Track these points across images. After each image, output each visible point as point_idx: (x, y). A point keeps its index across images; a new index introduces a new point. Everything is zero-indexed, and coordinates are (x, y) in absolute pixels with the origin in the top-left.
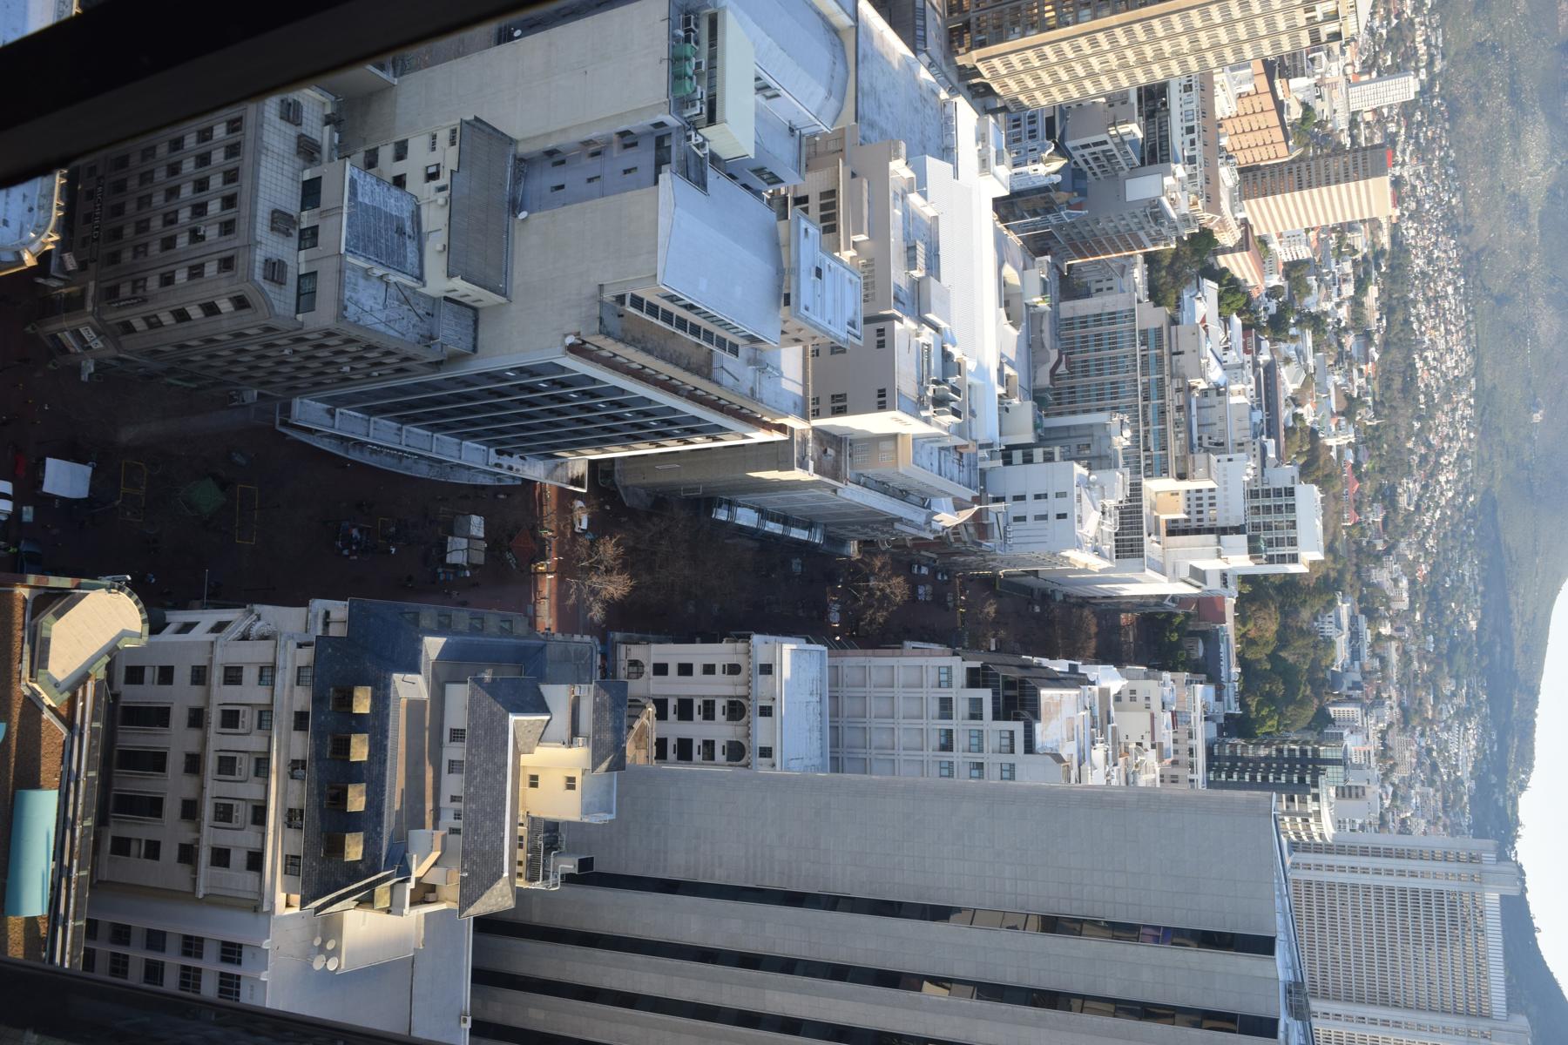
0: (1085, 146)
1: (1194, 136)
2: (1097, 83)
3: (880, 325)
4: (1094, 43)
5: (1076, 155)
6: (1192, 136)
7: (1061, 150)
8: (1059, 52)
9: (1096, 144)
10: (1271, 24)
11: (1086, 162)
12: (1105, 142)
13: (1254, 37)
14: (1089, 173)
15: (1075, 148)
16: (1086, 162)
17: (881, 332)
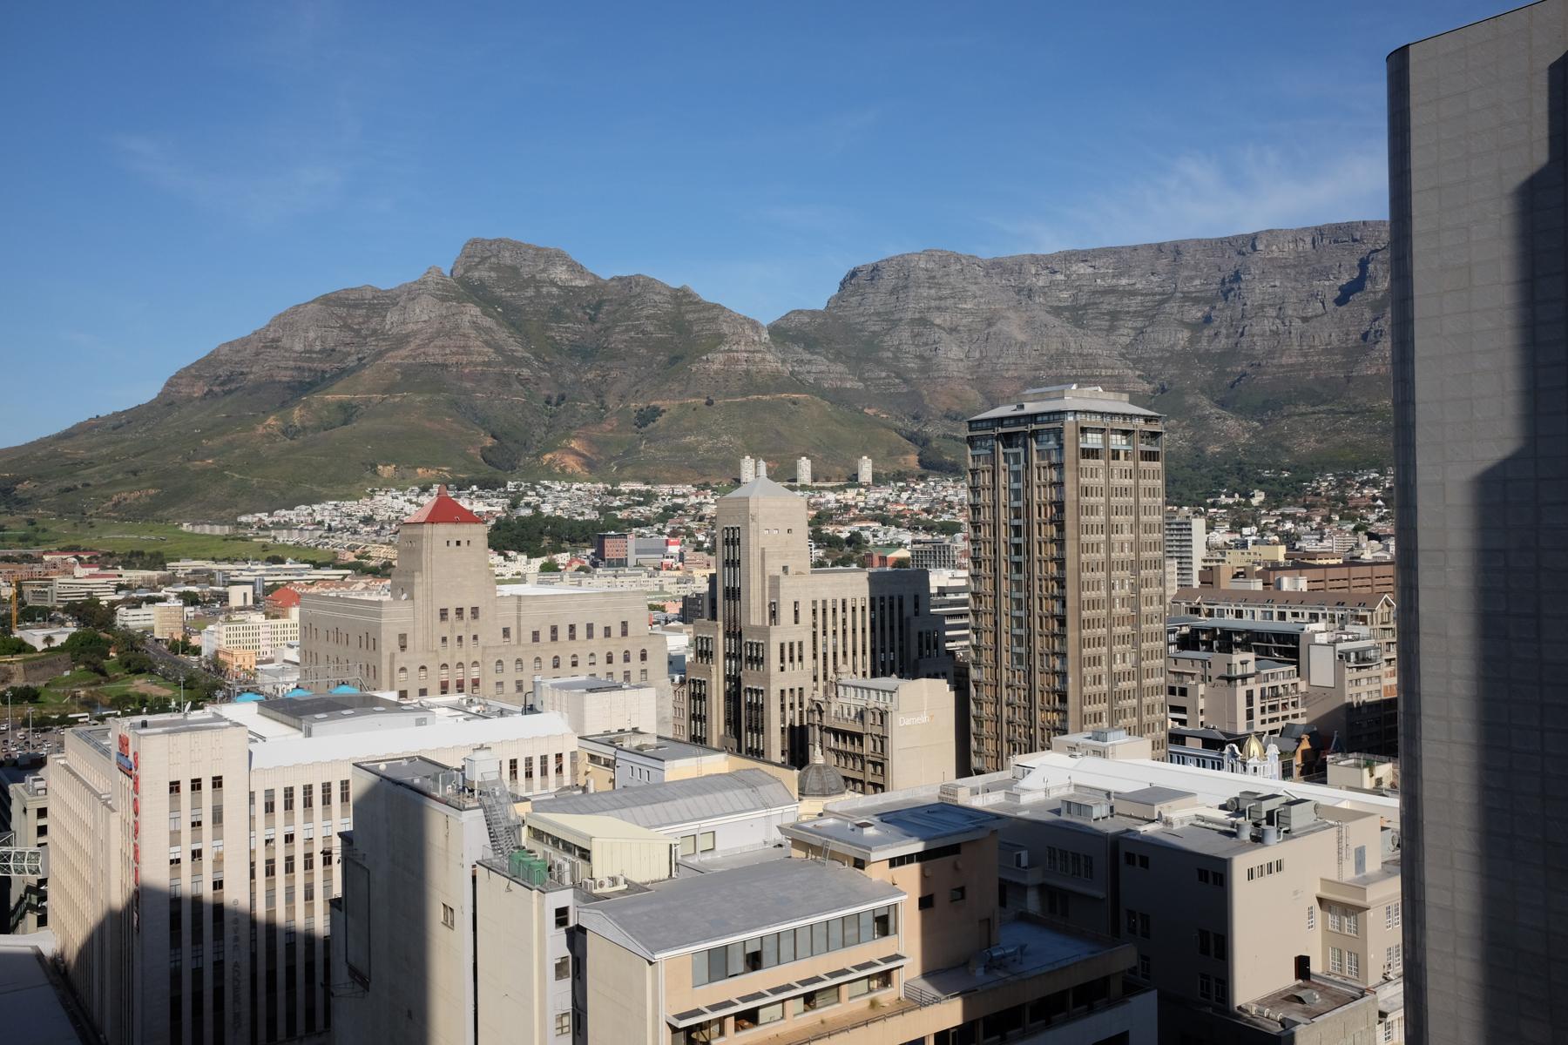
0: (1250, 715)
1: (1288, 613)
2: (1150, 673)
3: (1122, 860)
4: (1096, 661)
5: (1258, 727)
6: (1289, 615)
7: (1241, 741)
8: (1094, 699)
9: (1250, 701)
10: (1125, 491)
11: (1271, 720)
12: (1250, 695)
13: (1136, 510)
14: (1291, 721)
15: (1250, 726)
16: (1271, 720)
17: (1130, 858)
